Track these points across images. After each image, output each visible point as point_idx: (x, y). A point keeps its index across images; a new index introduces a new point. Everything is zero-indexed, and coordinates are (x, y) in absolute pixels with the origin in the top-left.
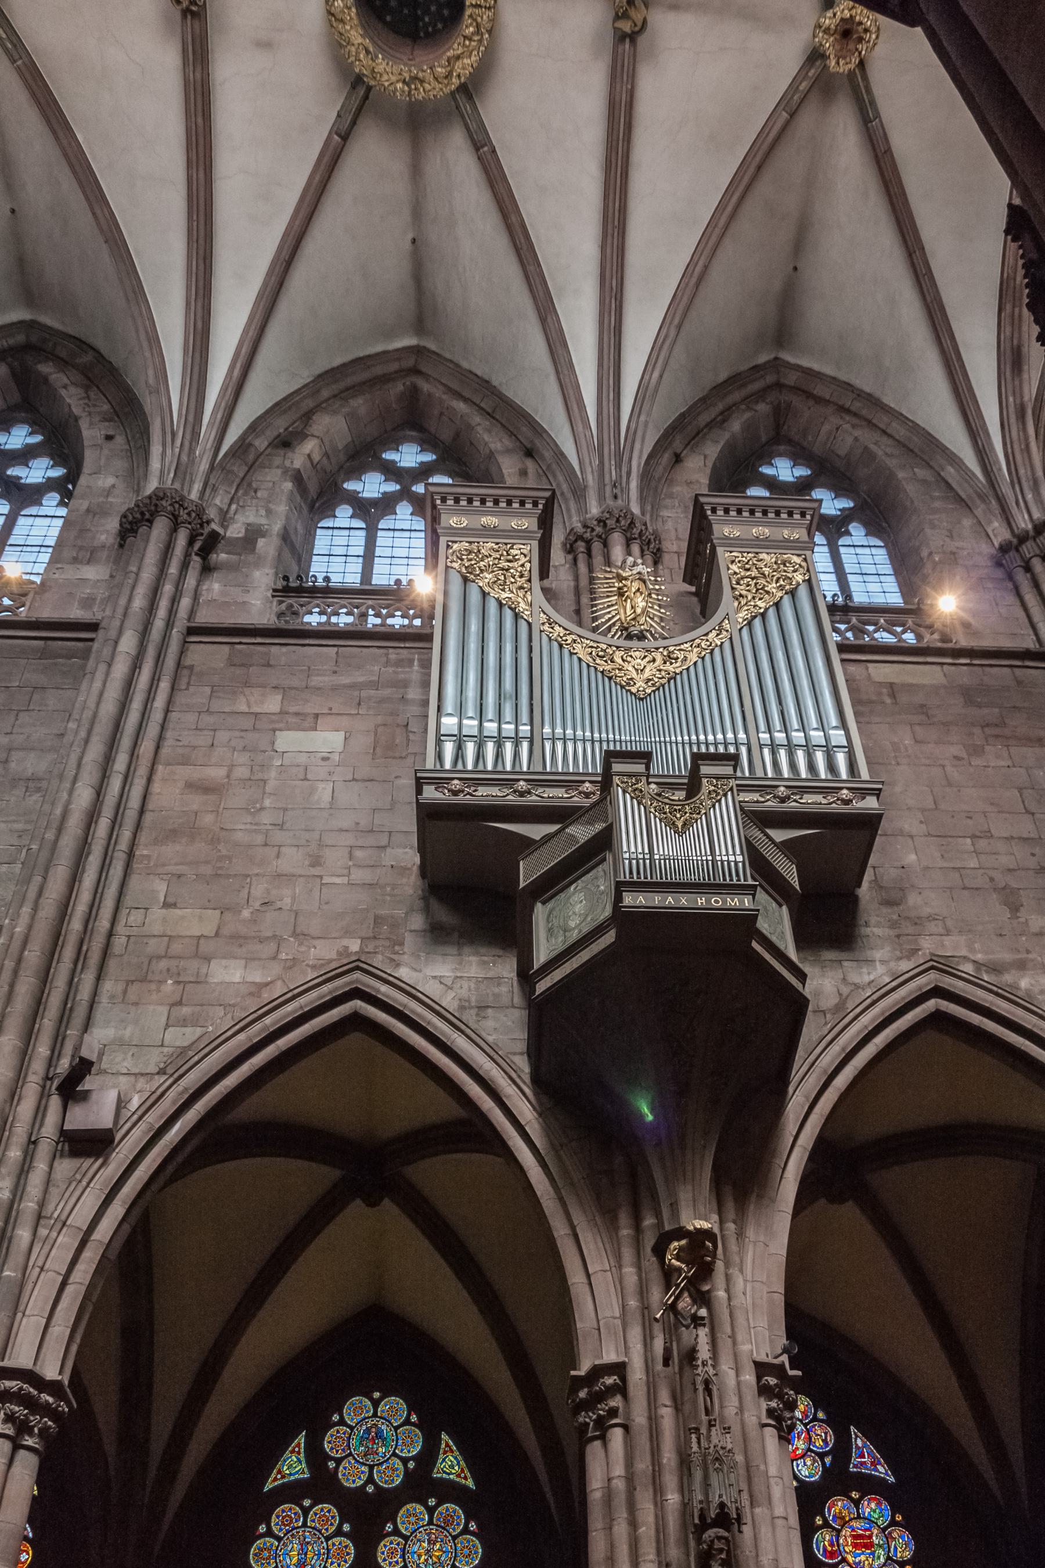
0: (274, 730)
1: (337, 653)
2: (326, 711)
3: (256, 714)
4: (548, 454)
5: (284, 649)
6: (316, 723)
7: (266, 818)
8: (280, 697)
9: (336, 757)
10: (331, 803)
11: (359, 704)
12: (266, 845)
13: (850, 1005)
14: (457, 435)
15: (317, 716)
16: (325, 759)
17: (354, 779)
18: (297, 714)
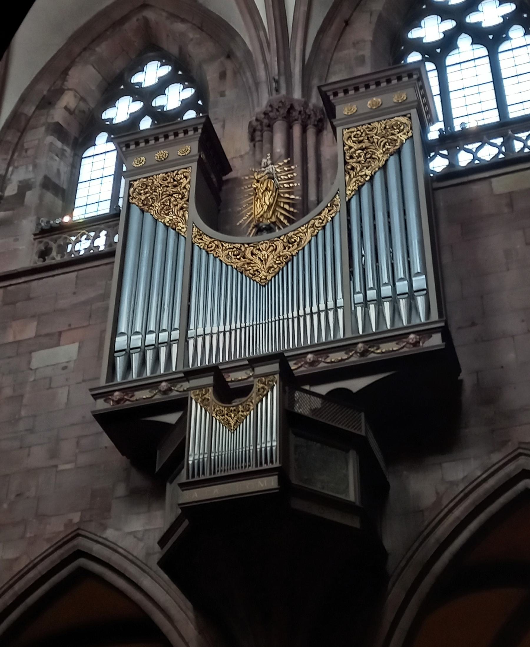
0: (30, 353)
1: (77, 277)
2: (66, 328)
3: (19, 342)
4: (239, 54)
5: (41, 282)
6: (59, 340)
7: (22, 426)
8: (35, 323)
9: (72, 365)
10: (67, 404)
11: (90, 316)
12: (21, 448)
13: (445, 502)
14: (181, 49)
15: (60, 333)
16: (64, 368)
17: (84, 381)
18: (47, 335)
